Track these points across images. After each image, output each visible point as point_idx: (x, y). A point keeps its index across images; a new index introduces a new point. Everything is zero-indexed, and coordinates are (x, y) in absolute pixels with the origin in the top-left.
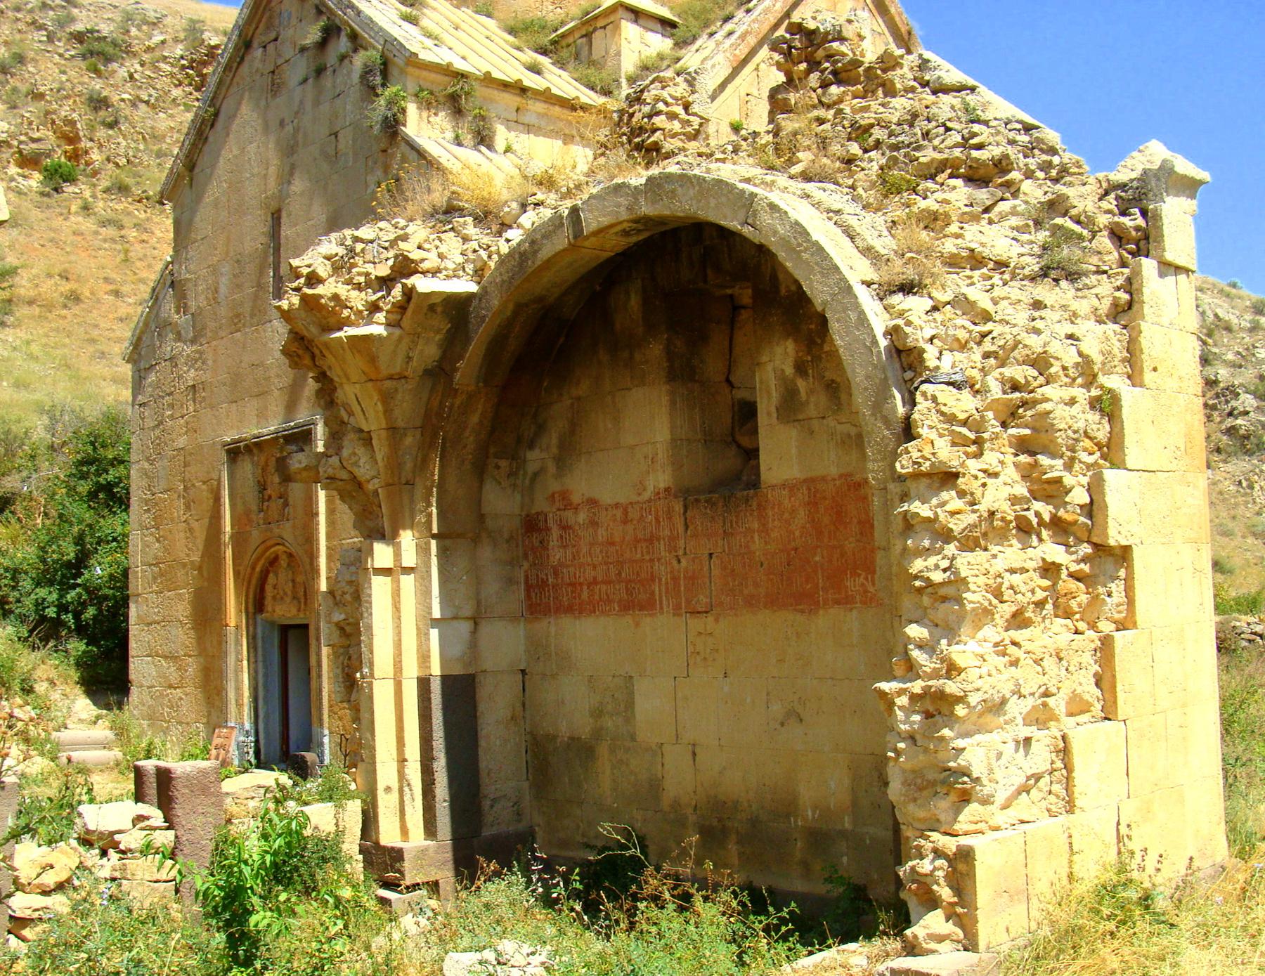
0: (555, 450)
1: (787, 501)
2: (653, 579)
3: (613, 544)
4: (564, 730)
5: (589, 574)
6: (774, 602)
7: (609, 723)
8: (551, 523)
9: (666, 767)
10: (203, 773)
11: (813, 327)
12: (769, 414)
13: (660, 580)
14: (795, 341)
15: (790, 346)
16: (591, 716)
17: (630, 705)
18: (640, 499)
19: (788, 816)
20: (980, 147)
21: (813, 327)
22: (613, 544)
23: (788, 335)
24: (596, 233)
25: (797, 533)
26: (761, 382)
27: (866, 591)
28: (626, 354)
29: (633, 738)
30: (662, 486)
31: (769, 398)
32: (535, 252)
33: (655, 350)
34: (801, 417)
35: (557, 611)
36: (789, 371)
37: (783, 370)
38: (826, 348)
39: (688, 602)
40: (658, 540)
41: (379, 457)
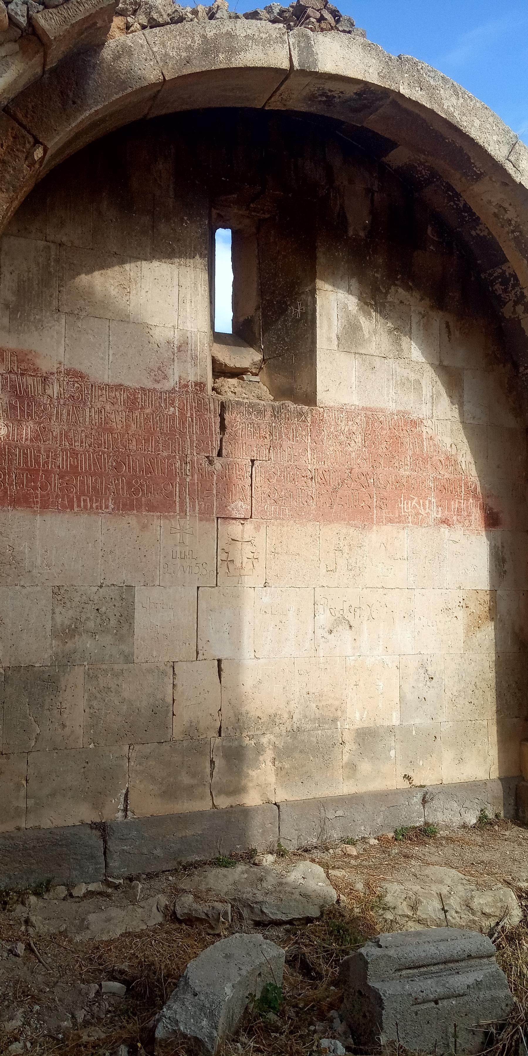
7: (87, 644)
9: (179, 688)
12: (329, 339)
13: (183, 480)
14: (360, 282)
15: (354, 283)
17: (127, 618)
18: (158, 386)
19: (335, 720)
22: (111, 431)
23: (352, 276)
27: (418, 514)
28: (146, 219)
29: (128, 658)
30: (192, 378)
31: (330, 327)
32: (232, 51)
34: (363, 351)
38: (389, 298)
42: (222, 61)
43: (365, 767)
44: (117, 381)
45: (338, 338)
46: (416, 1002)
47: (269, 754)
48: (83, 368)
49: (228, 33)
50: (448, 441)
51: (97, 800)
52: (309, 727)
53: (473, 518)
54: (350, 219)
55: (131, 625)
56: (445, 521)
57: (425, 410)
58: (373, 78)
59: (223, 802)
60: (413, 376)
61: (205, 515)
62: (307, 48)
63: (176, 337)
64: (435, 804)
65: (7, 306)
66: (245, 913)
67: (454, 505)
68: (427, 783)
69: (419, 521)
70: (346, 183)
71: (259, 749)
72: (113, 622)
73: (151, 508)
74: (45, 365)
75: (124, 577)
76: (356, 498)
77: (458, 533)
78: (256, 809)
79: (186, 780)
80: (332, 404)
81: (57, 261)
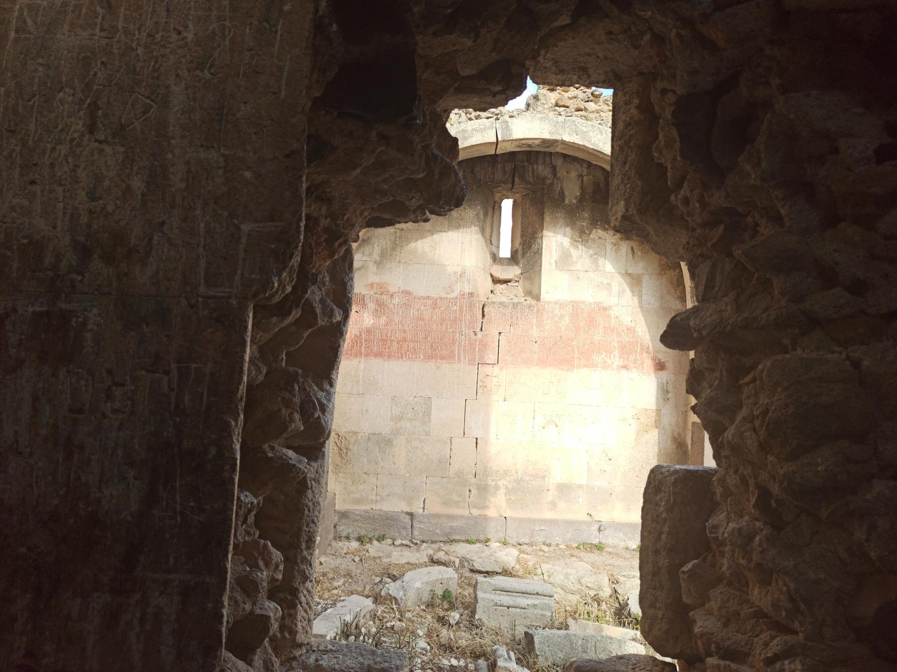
0: (376, 257)
4: (366, 428)
6: (542, 363)
8: (367, 300)
9: (453, 451)
12: (550, 264)
13: (460, 344)
15: (568, 230)
17: (428, 413)
18: (448, 296)
19: (544, 477)
22: (423, 320)
23: (568, 225)
27: (605, 362)
29: (427, 434)
30: (467, 291)
35: (367, 355)
38: (591, 236)
43: (562, 505)
44: (428, 295)
46: (496, 605)
47: (502, 491)
48: (410, 290)
49: (463, 130)
50: (629, 318)
51: (410, 501)
52: (528, 478)
53: (645, 365)
54: (567, 193)
55: (429, 417)
56: (625, 367)
57: (613, 301)
58: (546, 136)
59: (475, 512)
60: (605, 281)
61: (471, 362)
63: (459, 270)
64: (607, 532)
65: (375, 262)
66: (466, 564)
67: (632, 357)
68: (603, 519)
69: (605, 366)
70: (565, 174)
71: (497, 488)
72: (421, 415)
73: (443, 358)
74: (392, 289)
76: (566, 352)
77: (634, 374)
78: (492, 518)
79: (455, 497)
81: (400, 238)
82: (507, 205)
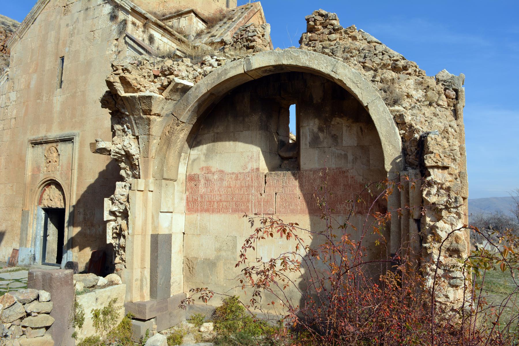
1: (312, 176)
2: (248, 201)
3: (231, 187)
4: (202, 255)
5: (218, 198)
7: (223, 254)
8: (200, 178)
10: (66, 275)
11: (327, 115)
12: (306, 144)
13: (252, 201)
14: (319, 120)
15: (317, 121)
16: (215, 250)
18: (244, 171)
20: (397, 60)
21: (327, 115)
22: (231, 187)
24: (256, 69)
25: (316, 188)
26: (303, 133)
27: (346, 210)
28: (241, 119)
31: (306, 139)
32: (226, 74)
33: (255, 118)
34: (320, 146)
35: (201, 211)
36: (316, 130)
37: (313, 130)
38: (333, 123)
39: (265, 210)
40: (252, 187)
41: (141, 146)
42: (223, 78)
44: (232, 172)
45: (309, 143)
49: (225, 69)
60: (343, 153)
62: (249, 63)
72: (231, 248)
75: (234, 233)
80: (307, 169)
82: (293, 109)
